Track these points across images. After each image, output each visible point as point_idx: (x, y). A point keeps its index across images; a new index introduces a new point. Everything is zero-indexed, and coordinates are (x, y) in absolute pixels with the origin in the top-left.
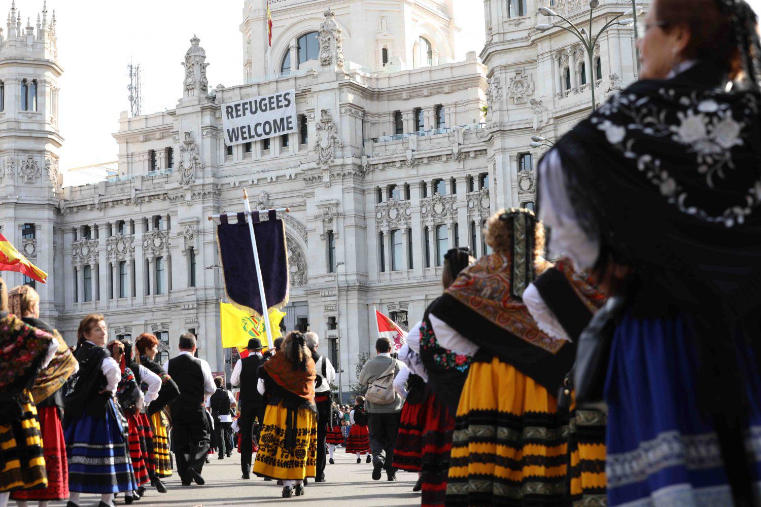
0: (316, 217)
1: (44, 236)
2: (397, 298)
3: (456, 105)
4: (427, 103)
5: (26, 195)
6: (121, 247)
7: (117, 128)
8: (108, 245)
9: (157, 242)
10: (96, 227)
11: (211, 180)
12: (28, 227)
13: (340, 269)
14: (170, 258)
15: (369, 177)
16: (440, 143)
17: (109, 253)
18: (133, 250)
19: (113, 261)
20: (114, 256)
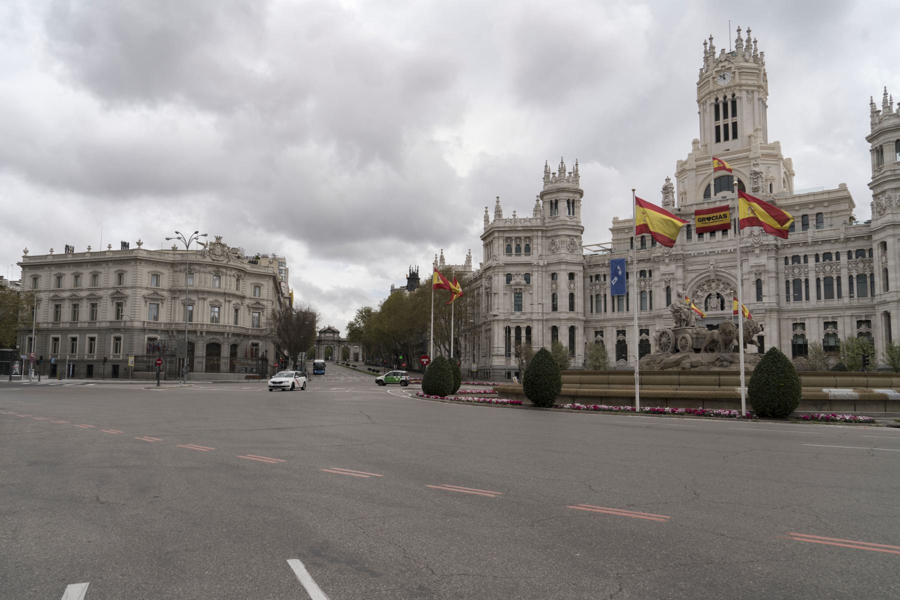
0: (750, 273)
1: (579, 279)
2: (799, 317)
3: (831, 213)
4: (811, 212)
5: (569, 258)
7: (611, 226)
9: (643, 284)
10: (605, 276)
11: (682, 252)
13: (765, 300)
14: (651, 292)
15: (781, 252)
16: (826, 232)
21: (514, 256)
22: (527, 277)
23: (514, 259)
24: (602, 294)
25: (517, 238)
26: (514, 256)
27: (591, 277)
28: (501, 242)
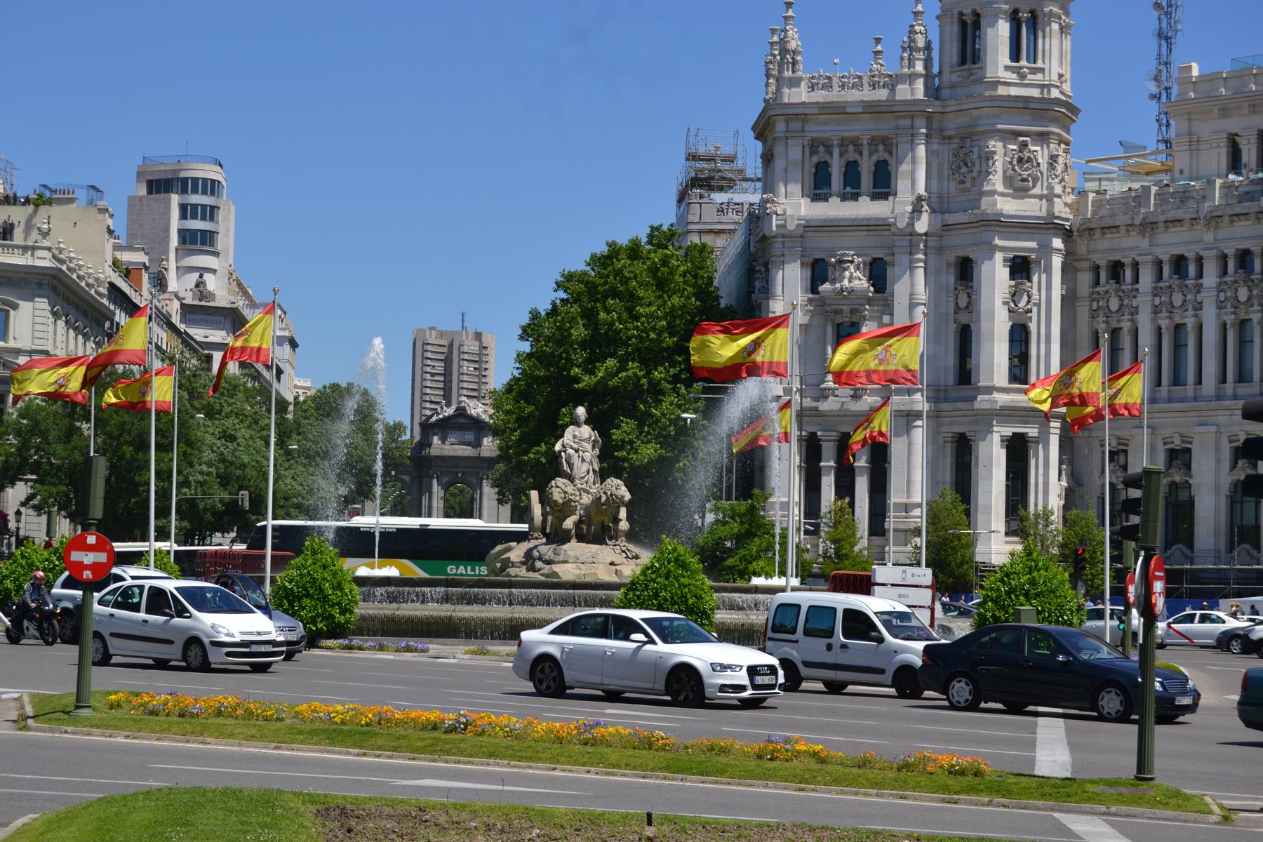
6: (1177, 299)
8: (1156, 295)
9: (1243, 294)
12: (1019, 261)
17: (1156, 310)
18: (1199, 307)
19: (1229, 319)
20: (1164, 314)
21: (834, 200)
22: (878, 274)
23: (835, 209)
24: (1126, 325)
25: (844, 143)
26: (834, 200)
27: (1096, 269)
28: (795, 152)
